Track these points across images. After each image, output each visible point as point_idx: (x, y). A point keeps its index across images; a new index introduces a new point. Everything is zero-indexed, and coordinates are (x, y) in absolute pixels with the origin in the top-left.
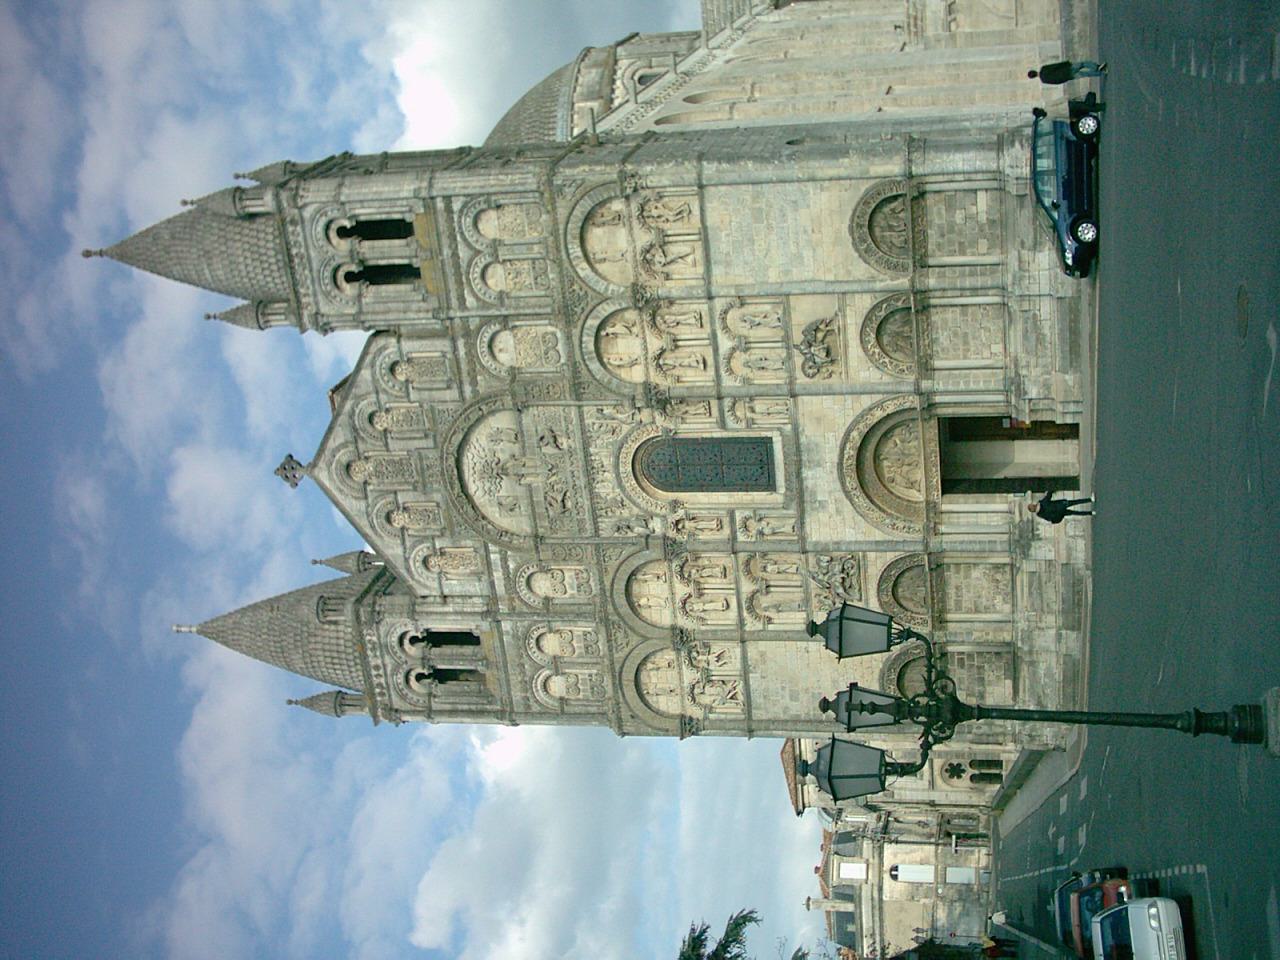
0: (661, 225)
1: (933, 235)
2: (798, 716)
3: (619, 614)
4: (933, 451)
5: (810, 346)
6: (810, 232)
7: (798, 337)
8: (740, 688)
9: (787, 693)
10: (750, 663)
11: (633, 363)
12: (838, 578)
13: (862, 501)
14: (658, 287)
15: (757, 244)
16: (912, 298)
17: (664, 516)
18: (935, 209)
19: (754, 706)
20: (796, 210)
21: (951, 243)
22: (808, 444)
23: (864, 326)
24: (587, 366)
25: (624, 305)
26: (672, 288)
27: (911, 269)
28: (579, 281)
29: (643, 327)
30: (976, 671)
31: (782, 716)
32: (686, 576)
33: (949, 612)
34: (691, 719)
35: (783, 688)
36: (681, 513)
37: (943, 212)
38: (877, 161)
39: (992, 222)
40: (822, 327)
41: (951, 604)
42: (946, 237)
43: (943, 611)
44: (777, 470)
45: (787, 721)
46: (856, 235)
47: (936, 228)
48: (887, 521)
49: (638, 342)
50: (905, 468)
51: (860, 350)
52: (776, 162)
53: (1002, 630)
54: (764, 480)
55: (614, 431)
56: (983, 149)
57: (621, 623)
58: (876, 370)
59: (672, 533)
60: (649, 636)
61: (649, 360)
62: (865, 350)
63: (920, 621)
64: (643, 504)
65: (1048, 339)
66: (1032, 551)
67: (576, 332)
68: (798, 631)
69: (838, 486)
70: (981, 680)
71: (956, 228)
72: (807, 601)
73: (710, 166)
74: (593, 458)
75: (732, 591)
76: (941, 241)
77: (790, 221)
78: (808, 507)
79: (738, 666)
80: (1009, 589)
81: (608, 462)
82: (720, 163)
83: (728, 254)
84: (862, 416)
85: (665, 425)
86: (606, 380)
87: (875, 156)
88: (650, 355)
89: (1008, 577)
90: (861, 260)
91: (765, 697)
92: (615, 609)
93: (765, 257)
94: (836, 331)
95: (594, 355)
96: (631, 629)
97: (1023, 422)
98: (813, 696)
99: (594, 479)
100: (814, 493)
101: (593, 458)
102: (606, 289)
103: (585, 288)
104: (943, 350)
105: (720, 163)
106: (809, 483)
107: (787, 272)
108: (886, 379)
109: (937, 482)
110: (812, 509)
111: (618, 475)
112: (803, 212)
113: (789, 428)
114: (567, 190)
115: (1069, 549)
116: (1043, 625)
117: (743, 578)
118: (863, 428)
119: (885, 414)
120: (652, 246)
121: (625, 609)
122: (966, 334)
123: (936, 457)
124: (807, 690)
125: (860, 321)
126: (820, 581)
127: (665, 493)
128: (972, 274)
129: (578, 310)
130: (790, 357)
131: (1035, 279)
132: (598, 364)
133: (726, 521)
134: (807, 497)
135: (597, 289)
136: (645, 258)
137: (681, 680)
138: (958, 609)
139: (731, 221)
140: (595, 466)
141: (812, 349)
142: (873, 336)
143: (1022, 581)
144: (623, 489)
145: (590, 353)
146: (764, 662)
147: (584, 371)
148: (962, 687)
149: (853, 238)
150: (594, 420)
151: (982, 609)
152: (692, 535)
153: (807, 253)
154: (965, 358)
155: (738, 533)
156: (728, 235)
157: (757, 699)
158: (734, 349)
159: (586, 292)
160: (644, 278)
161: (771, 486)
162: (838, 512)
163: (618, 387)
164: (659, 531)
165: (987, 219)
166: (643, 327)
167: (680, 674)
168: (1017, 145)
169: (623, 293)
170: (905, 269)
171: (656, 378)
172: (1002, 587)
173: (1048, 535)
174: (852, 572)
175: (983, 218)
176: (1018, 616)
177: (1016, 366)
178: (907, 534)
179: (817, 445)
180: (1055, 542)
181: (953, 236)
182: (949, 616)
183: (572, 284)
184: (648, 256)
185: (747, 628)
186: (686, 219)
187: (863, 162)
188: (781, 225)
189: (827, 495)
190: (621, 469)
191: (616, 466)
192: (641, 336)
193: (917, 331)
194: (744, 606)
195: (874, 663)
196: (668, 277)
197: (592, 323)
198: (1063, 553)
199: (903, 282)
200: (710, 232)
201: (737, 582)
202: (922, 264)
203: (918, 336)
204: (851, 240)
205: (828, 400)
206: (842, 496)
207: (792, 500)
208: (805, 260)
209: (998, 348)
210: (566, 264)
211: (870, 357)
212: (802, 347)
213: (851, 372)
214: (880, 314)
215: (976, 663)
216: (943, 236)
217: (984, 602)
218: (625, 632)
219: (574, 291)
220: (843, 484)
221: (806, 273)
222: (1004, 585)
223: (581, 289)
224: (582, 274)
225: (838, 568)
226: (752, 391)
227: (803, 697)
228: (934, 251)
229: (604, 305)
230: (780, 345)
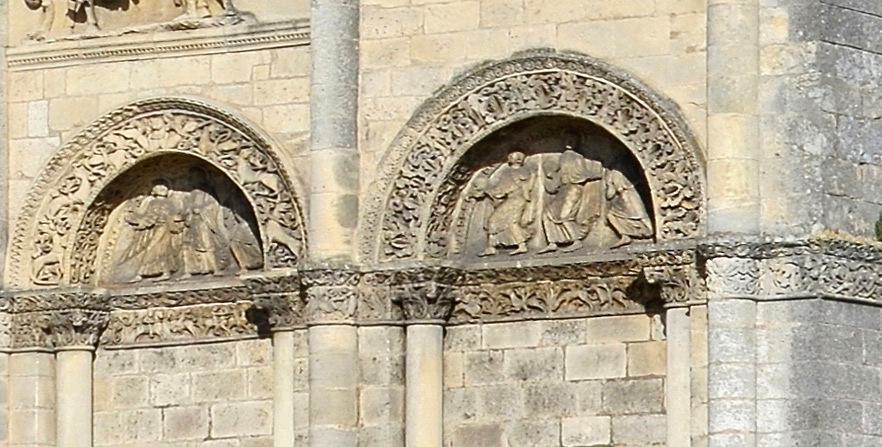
18: (615, 344)
21: (497, 400)
23: (204, 113)
37: (608, 372)
38: (773, 142)
42: (517, 383)
46: (515, 77)
51: (122, 101)
58: (48, 157)
62: (121, 117)
71: (545, 418)
76: (507, 365)
104: (133, 383)
149: (502, 65)
181: (519, 408)
187: (768, 93)
193: (198, 295)
203: (179, 299)
204: (498, 57)
213: (40, 76)
214: (243, 165)
216: (523, 374)
228: (471, 344)
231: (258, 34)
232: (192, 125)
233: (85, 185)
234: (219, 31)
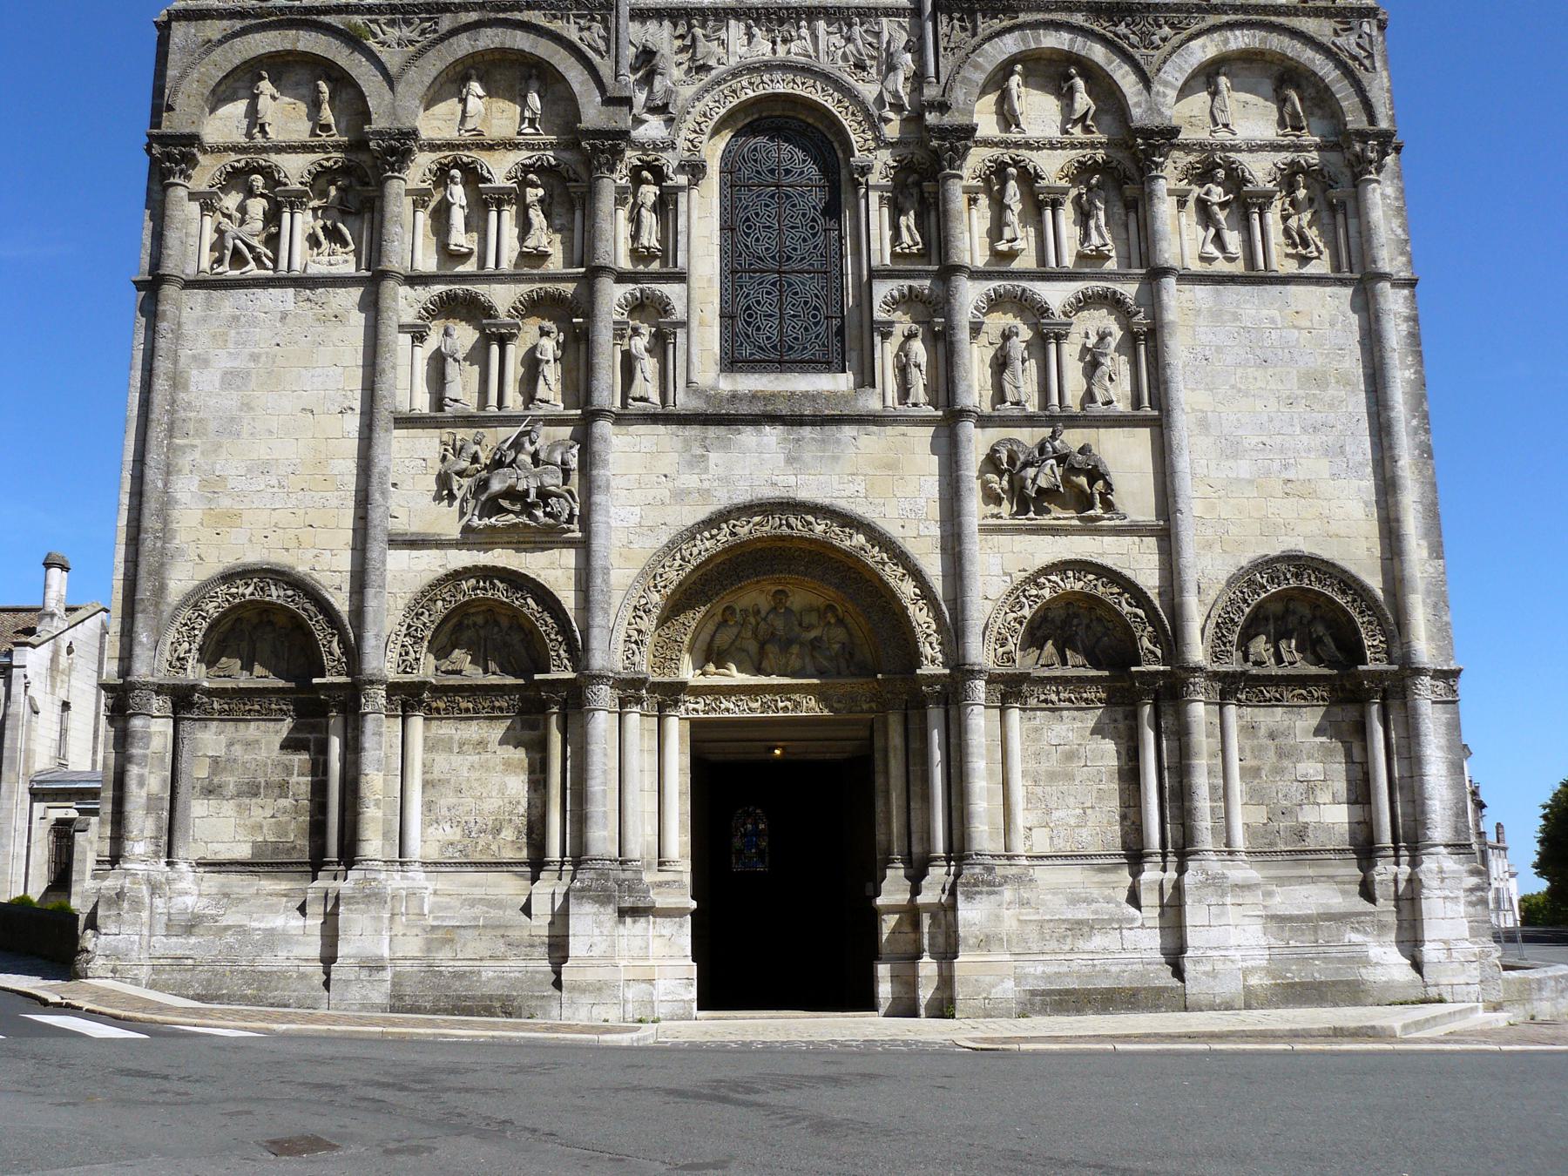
0: (1277, 204)
1: (1270, 718)
2: (186, 388)
3: (454, 32)
4: (797, 705)
5: (1062, 459)
6: (1286, 475)
7: (1072, 439)
8: (252, 270)
9: (240, 364)
10: (321, 290)
11: (1008, 118)
12: (529, 484)
13: (706, 546)
14: (1169, 177)
15: (1259, 373)
16: (1162, 668)
17: (673, 146)
19: (216, 294)
20: (1326, 453)
21: (1258, 751)
22: (838, 441)
23: (1102, 571)
24: (1009, 30)
25: (1136, 112)
26: (1165, 208)
27: (1216, 667)
28: (1176, 40)
29: (1082, 145)
30: (276, 778)
31: (185, 353)
32: (532, 176)
33: (427, 728)
34: (192, 161)
35: (255, 358)
36: (682, 180)
39: (1301, 833)
40: (1100, 484)
41: (445, 729)
43: (432, 714)
44: (772, 376)
45: (175, 362)
47: (1286, 723)
48: (656, 597)
49: (1054, 133)
50: (753, 647)
52: (1415, 422)
53: (386, 835)
54: (746, 351)
55: (864, 68)
56: (1457, 815)
57: (431, 36)
59: (632, 156)
60: (400, 88)
61: (1012, 151)
63: (412, 654)
64: (700, 106)
65: (1081, 944)
66: (589, 908)
67: (1078, 19)
68: (393, 396)
69: (742, 496)
70: (253, 790)
71: (1286, 763)
72: (468, 421)
73: (1401, 301)
74: (803, 23)
75: (491, 263)
76: (1263, 731)
77: (1305, 438)
78: (693, 431)
79: (313, 270)
80: (477, 857)
81: (797, 50)
82: (1407, 319)
83: (1236, 317)
84: (900, 557)
85: (878, 166)
86: (980, 60)
87: (1435, 606)
88: (1025, 154)
89: (508, 854)
90: (1234, 570)
91: (236, 318)
92: (468, 27)
93: (1233, 387)
94: (1091, 512)
95: (1033, 46)
96: (421, 53)
97: (878, 894)
98: (232, 419)
99: (757, 21)
100: (725, 446)
101: (803, 23)
102: (1166, 84)
103: (1168, 47)
104: (1036, 730)
105: (1407, 319)
106: (748, 436)
107: (1203, 425)
108: (988, 607)
109: (728, 710)
110: (686, 441)
111: (768, 67)
112: (1322, 467)
113: (871, 402)
114: (1353, 39)
115: (598, 988)
116: (399, 929)
117: (525, 288)
118: (873, 556)
119: (907, 603)
120: (1245, 181)
121: (463, 45)
122: (1070, 777)
123: (785, 709)
124: (247, 406)
125: (1108, 562)
126: (517, 445)
127: (719, 153)
128: (1213, 788)
129: (1122, 29)
130: (1030, 421)
131: (1218, 916)
132: (1015, 50)
133: (655, 266)
134: (713, 431)
135: (1166, 68)
136: (1220, 166)
137: (280, 149)
138: (430, 746)
139: (1299, 328)
140: (786, 27)
141: (1053, 461)
142: (1078, 586)
143: (496, 886)
144: (735, 74)
145: (1037, 40)
146: (322, 320)
147: (997, 24)
148: (237, 750)
150: (885, 37)
151: (432, 794)
152: (620, 202)
153: (1244, 468)
154: (1024, 774)
155: (632, 286)
156: (1273, 321)
157: (229, 301)
158: (1044, 311)
159: (1158, 48)
160: (1182, 159)
161: (732, 362)
162: (680, 495)
163: (966, 80)
164: (639, 134)
165: (1306, 826)
166: (1082, 145)
167: (305, 148)
168: (1474, 881)
169: (1160, 113)
170: (1216, 657)
171: (976, 160)
172: (481, 843)
173: (623, 942)
174: (539, 513)
175: (1308, 815)
176: (418, 877)
177: (1019, 880)
178: (623, 636)
179: (835, 459)
180: (609, 959)
181: (1271, 757)
182: (417, 723)
183: (1172, 26)
184: (1221, 173)
185: (404, 290)
186: (1290, 250)
188: (1296, 421)
189: (721, 471)
190: (778, 75)
191: (785, 67)
192: (1066, 139)
194: (457, 288)
195: (310, 554)
196: (1182, 204)
197: (1098, 53)
198: (591, 976)
199: (1197, 652)
200: (1280, 288)
201: (514, 278)
202: (1230, 688)
205: (930, 487)
206: (722, 499)
207: (707, 403)
208: (1231, 463)
209: (1041, 845)
210: (1212, 20)
211: (1033, 580)
212: (1057, 443)
214: (1124, 603)
215: (294, 779)
217: (446, 800)
218: (411, 42)
219: (1160, 27)
220: (748, 510)
221: (1204, 462)
222: (488, 846)
223: (1164, 40)
224: (1195, 44)
225: (553, 480)
226: (963, 334)
227: (231, 400)
229: (1132, 78)
230: (1055, 400)
231: (1135, 530)
232: (1091, 577)
233: (1027, 607)
234: (1112, 523)
